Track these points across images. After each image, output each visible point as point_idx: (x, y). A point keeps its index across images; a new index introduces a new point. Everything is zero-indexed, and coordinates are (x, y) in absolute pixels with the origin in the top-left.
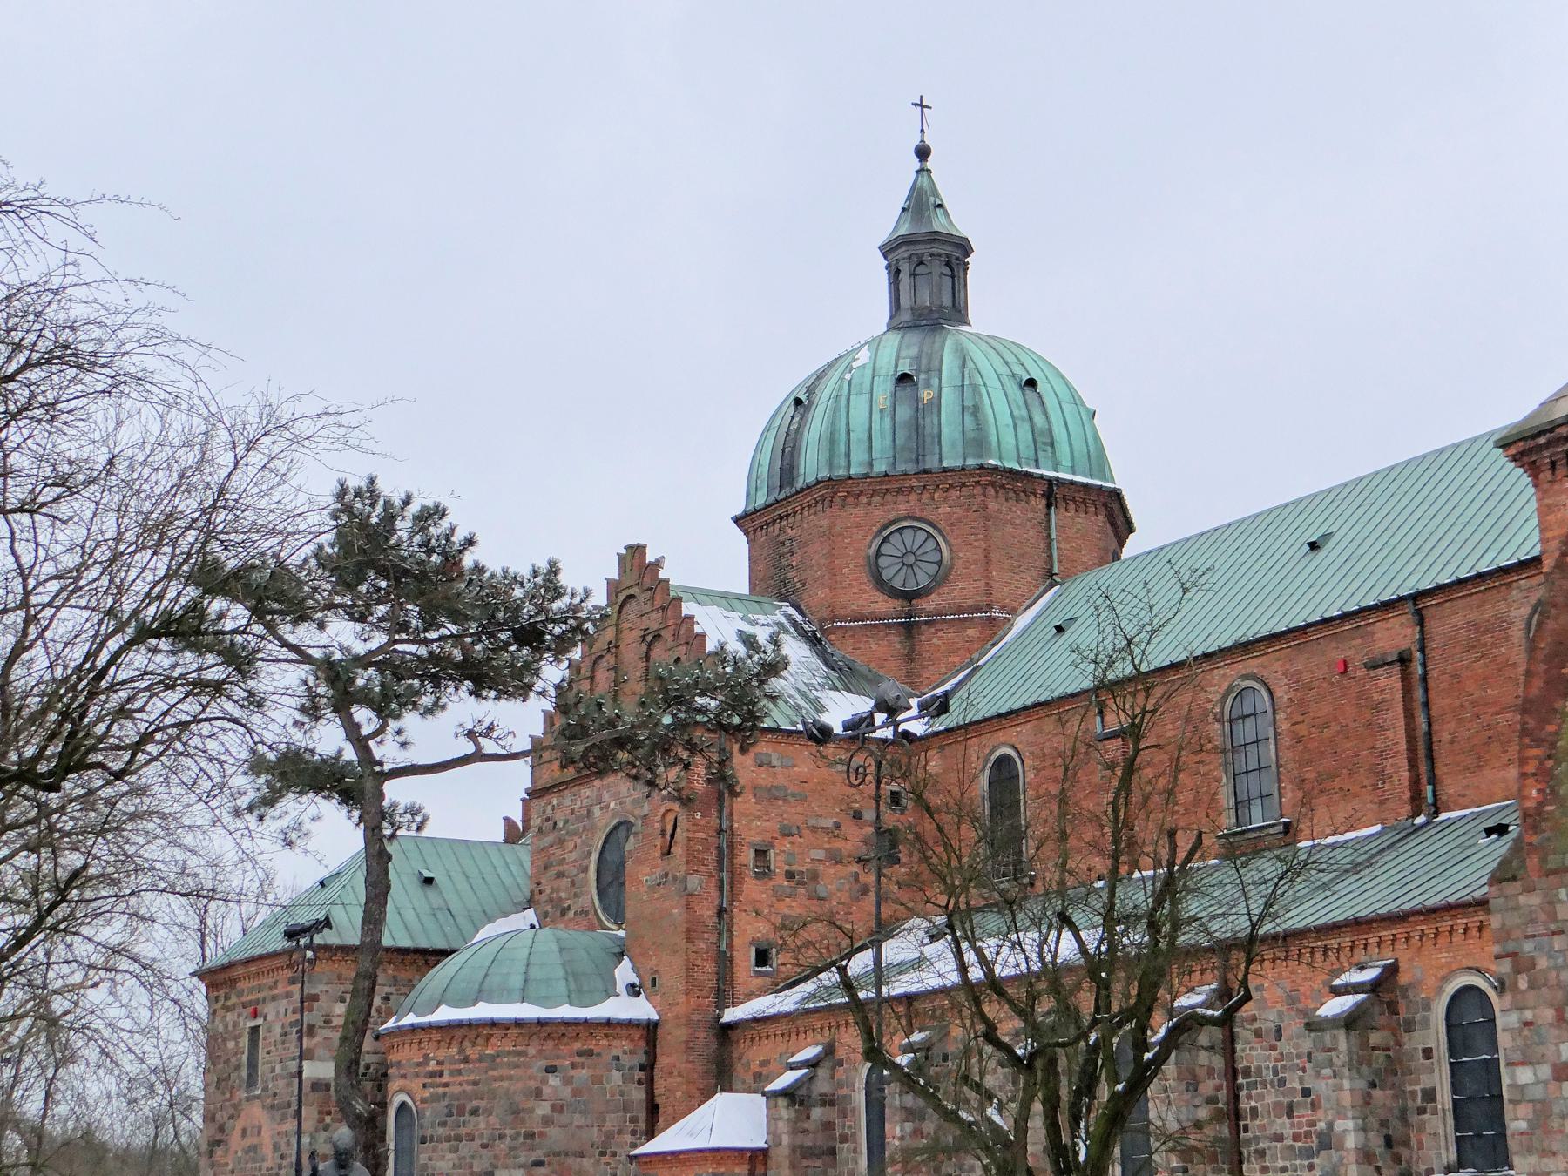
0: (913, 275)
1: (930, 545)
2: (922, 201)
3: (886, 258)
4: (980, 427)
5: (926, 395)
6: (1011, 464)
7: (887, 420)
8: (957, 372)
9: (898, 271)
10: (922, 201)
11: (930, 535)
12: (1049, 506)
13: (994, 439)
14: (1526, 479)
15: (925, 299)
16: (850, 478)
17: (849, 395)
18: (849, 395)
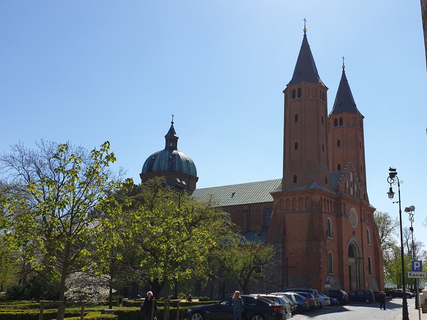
0: (170, 141)
1: (172, 183)
2: (172, 131)
3: (165, 137)
4: (181, 167)
5: (173, 161)
6: (185, 173)
7: (167, 164)
8: (178, 158)
9: (168, 140)
10: (172, 131)
11: (172, 182)
12: (189, 179)
13: (183, 169)
14: (272, 197)
15: (171, 145)
16: (161, 172)
17: (162, 159)
18: (162, 159)
